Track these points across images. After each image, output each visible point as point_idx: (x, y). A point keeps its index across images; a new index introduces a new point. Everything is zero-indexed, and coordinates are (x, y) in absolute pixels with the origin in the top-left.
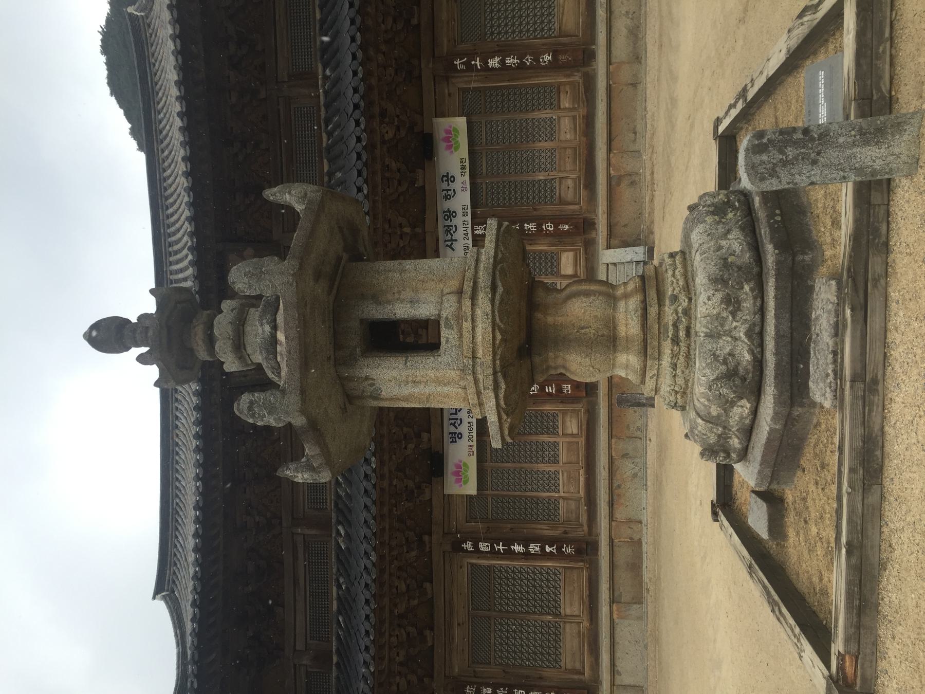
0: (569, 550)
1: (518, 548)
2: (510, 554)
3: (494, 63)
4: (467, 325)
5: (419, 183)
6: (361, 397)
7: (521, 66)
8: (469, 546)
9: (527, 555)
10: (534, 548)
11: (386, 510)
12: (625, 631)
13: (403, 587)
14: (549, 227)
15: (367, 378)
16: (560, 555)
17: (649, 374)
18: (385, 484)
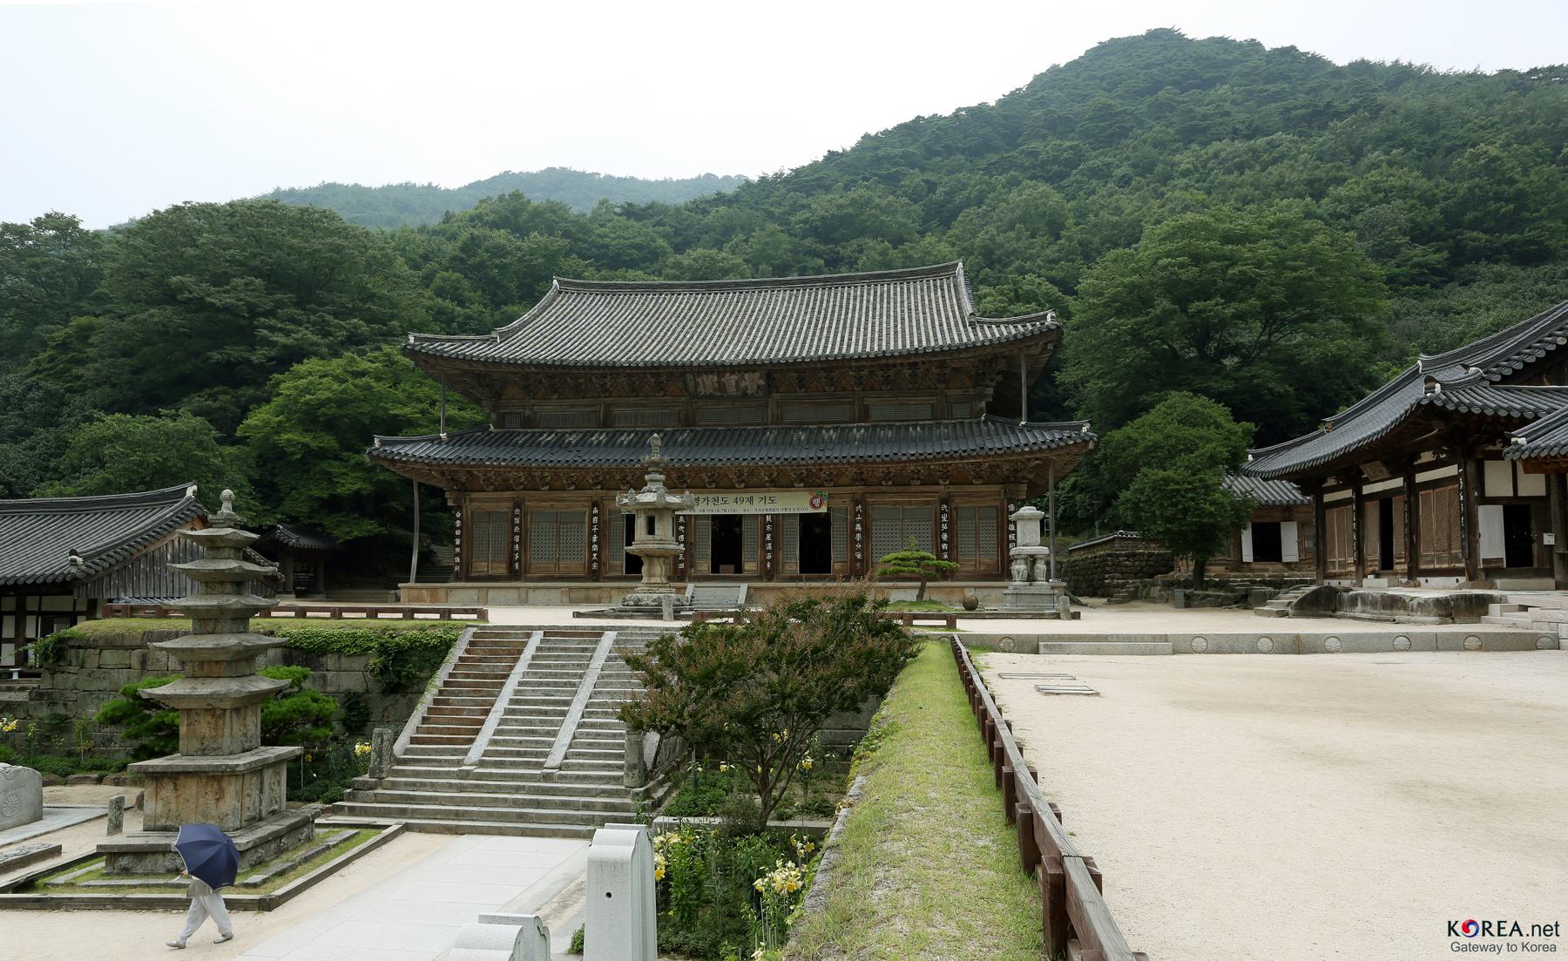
0: (595, 566)
1: (595, 538)
2: (591, 534)
3: (858, 527)
8: (595, 511)
9: (591, 543)
10: (595, 547)
12: (556, 594)
16: (591, 562)
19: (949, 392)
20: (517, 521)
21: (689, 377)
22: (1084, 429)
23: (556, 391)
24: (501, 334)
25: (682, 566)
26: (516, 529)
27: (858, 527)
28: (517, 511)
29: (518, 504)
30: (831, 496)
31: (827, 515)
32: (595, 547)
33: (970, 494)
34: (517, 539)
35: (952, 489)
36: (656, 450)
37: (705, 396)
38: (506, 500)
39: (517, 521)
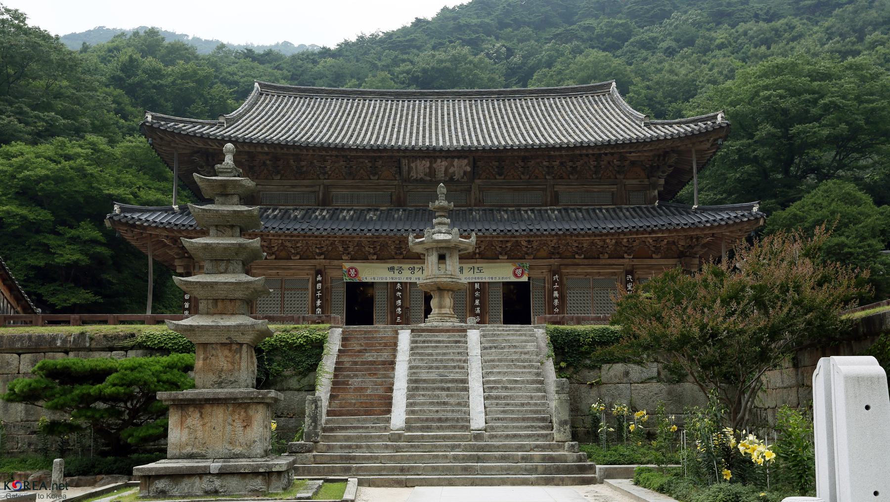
1: (319, 302)
2: (316, 298)
3: (556, 294)
7: (554, 307)
8: (319, 278)
19: (627, 182)
21: (404, 162)
22: (755, 209)
23: (278, 173)
24: (226, 119)
27: (556, 294)
30: (531, 268)
31: (526, 285)
35: (636, 262)
36: (442, 197)
37: (416, 180)
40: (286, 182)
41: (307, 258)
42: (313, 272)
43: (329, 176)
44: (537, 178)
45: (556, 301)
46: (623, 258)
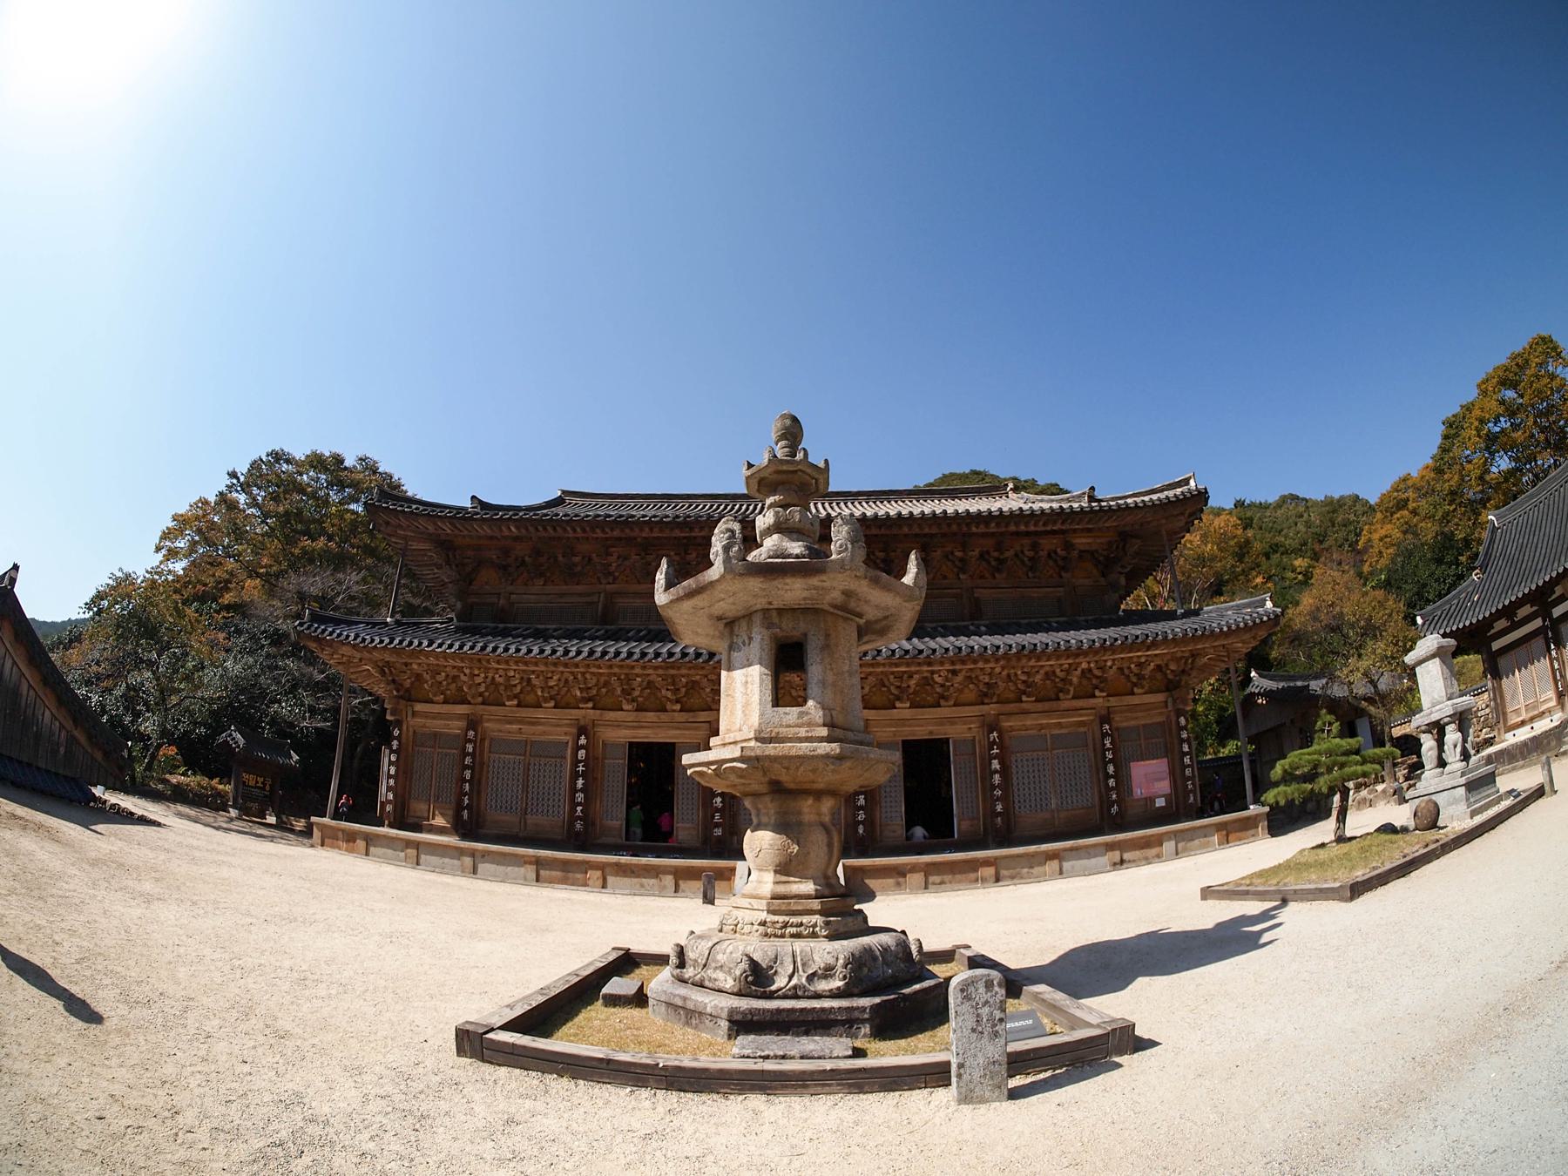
0: (578, 825)
1: (580, 782)
3: (996, 764)
4: (802, 732)
5: (898, 704)
6: (732, 633)
8: (583, 741)
10: (580, 797)
11: (616, 670)
13: (552, 683)
14: (861, 816)
15: (750, 639)
16: (573, 818)
17: (753, 901)
18: (637, 671)
20: (470, 748)
23: (542, 575)
25: (718, 832)
26: (468, 760)
28: (471, 733)
29: (473, 723)
32: (580, 797)
33: (1133, 708)
34: (468, 774)
35: (1113, 701)
38: (460, 717)
39: (470, 748)
40: (550, 588)
41: (567, 707)
42: (574, 731)
43: (615, 579)
44: (945, 577)
45: (997, 776)
46: (1094, 696)
